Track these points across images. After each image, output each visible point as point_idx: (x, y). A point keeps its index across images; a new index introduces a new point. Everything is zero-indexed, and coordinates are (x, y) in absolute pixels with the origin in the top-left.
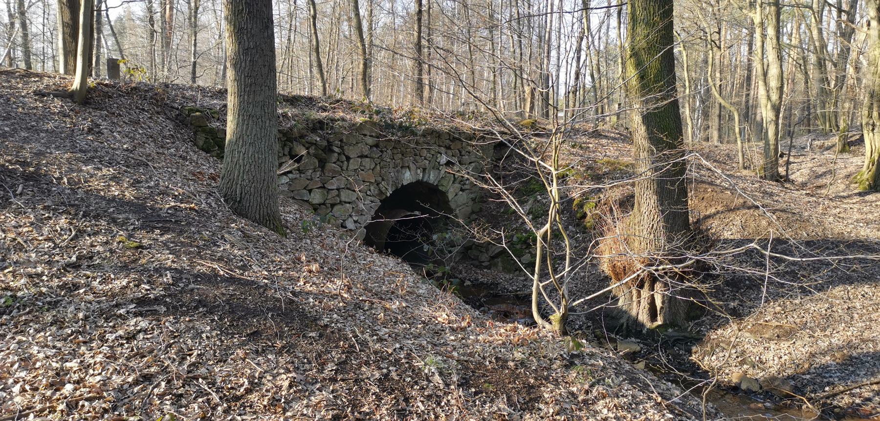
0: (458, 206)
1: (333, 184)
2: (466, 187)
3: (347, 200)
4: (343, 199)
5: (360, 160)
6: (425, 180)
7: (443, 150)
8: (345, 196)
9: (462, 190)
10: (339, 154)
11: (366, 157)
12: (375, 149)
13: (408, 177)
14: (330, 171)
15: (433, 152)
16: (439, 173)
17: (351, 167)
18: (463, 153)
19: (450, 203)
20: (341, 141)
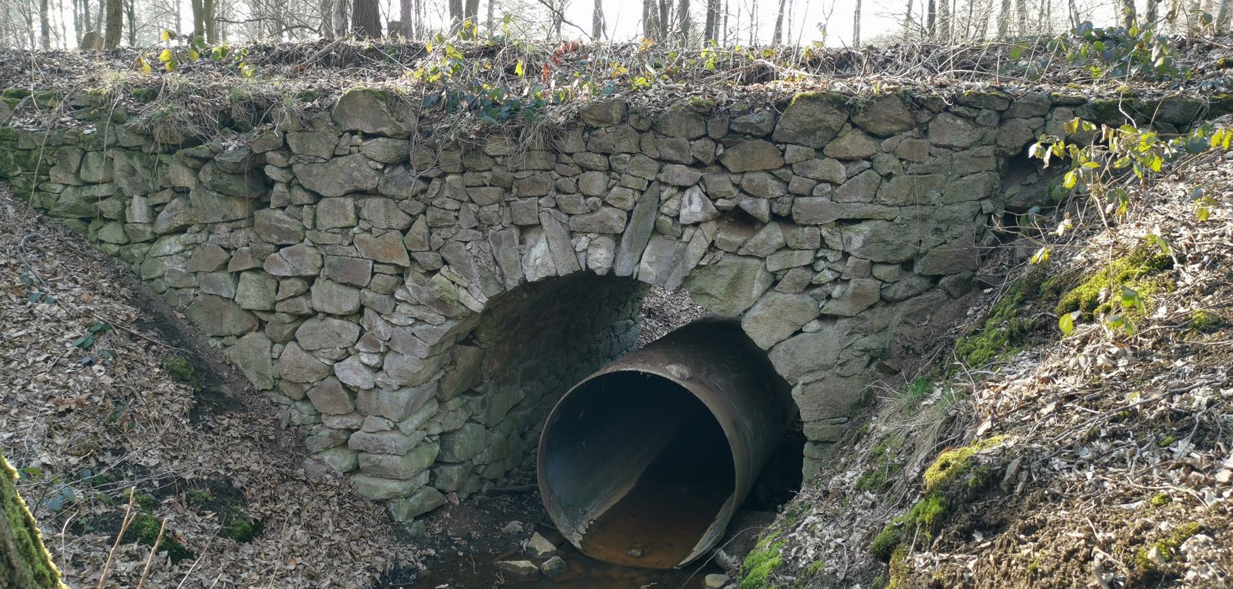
0: (798, 371)
1: (281, 264)
2: (831, 307)
3: (328, 309)
4: (317, 305)
5: (349, 202)
6: (622, 270)
7: (681, 174)
8: (320, 297)
9: (822, 318)
10: (289, 185)
11: (375, 193)
12: (400, 170)
13: (541, 259)
14: (270, 229)
15: (632, 182)
16: (682, 253)
17: (325, 221)
18: (796, 184)
19: (772, 357)
20: (285, 148)
